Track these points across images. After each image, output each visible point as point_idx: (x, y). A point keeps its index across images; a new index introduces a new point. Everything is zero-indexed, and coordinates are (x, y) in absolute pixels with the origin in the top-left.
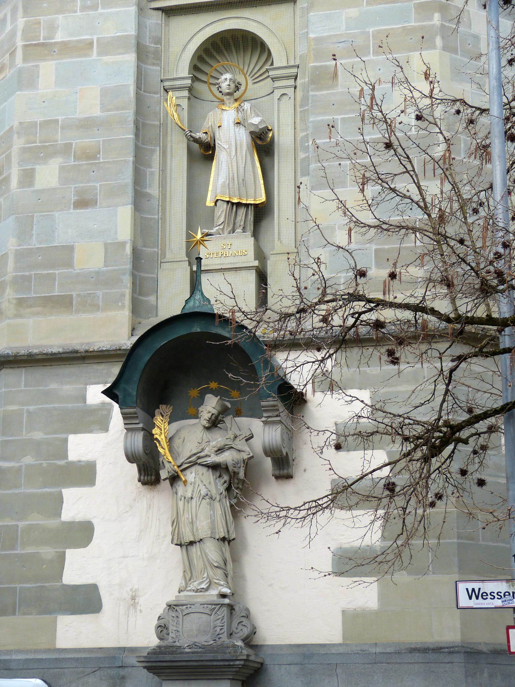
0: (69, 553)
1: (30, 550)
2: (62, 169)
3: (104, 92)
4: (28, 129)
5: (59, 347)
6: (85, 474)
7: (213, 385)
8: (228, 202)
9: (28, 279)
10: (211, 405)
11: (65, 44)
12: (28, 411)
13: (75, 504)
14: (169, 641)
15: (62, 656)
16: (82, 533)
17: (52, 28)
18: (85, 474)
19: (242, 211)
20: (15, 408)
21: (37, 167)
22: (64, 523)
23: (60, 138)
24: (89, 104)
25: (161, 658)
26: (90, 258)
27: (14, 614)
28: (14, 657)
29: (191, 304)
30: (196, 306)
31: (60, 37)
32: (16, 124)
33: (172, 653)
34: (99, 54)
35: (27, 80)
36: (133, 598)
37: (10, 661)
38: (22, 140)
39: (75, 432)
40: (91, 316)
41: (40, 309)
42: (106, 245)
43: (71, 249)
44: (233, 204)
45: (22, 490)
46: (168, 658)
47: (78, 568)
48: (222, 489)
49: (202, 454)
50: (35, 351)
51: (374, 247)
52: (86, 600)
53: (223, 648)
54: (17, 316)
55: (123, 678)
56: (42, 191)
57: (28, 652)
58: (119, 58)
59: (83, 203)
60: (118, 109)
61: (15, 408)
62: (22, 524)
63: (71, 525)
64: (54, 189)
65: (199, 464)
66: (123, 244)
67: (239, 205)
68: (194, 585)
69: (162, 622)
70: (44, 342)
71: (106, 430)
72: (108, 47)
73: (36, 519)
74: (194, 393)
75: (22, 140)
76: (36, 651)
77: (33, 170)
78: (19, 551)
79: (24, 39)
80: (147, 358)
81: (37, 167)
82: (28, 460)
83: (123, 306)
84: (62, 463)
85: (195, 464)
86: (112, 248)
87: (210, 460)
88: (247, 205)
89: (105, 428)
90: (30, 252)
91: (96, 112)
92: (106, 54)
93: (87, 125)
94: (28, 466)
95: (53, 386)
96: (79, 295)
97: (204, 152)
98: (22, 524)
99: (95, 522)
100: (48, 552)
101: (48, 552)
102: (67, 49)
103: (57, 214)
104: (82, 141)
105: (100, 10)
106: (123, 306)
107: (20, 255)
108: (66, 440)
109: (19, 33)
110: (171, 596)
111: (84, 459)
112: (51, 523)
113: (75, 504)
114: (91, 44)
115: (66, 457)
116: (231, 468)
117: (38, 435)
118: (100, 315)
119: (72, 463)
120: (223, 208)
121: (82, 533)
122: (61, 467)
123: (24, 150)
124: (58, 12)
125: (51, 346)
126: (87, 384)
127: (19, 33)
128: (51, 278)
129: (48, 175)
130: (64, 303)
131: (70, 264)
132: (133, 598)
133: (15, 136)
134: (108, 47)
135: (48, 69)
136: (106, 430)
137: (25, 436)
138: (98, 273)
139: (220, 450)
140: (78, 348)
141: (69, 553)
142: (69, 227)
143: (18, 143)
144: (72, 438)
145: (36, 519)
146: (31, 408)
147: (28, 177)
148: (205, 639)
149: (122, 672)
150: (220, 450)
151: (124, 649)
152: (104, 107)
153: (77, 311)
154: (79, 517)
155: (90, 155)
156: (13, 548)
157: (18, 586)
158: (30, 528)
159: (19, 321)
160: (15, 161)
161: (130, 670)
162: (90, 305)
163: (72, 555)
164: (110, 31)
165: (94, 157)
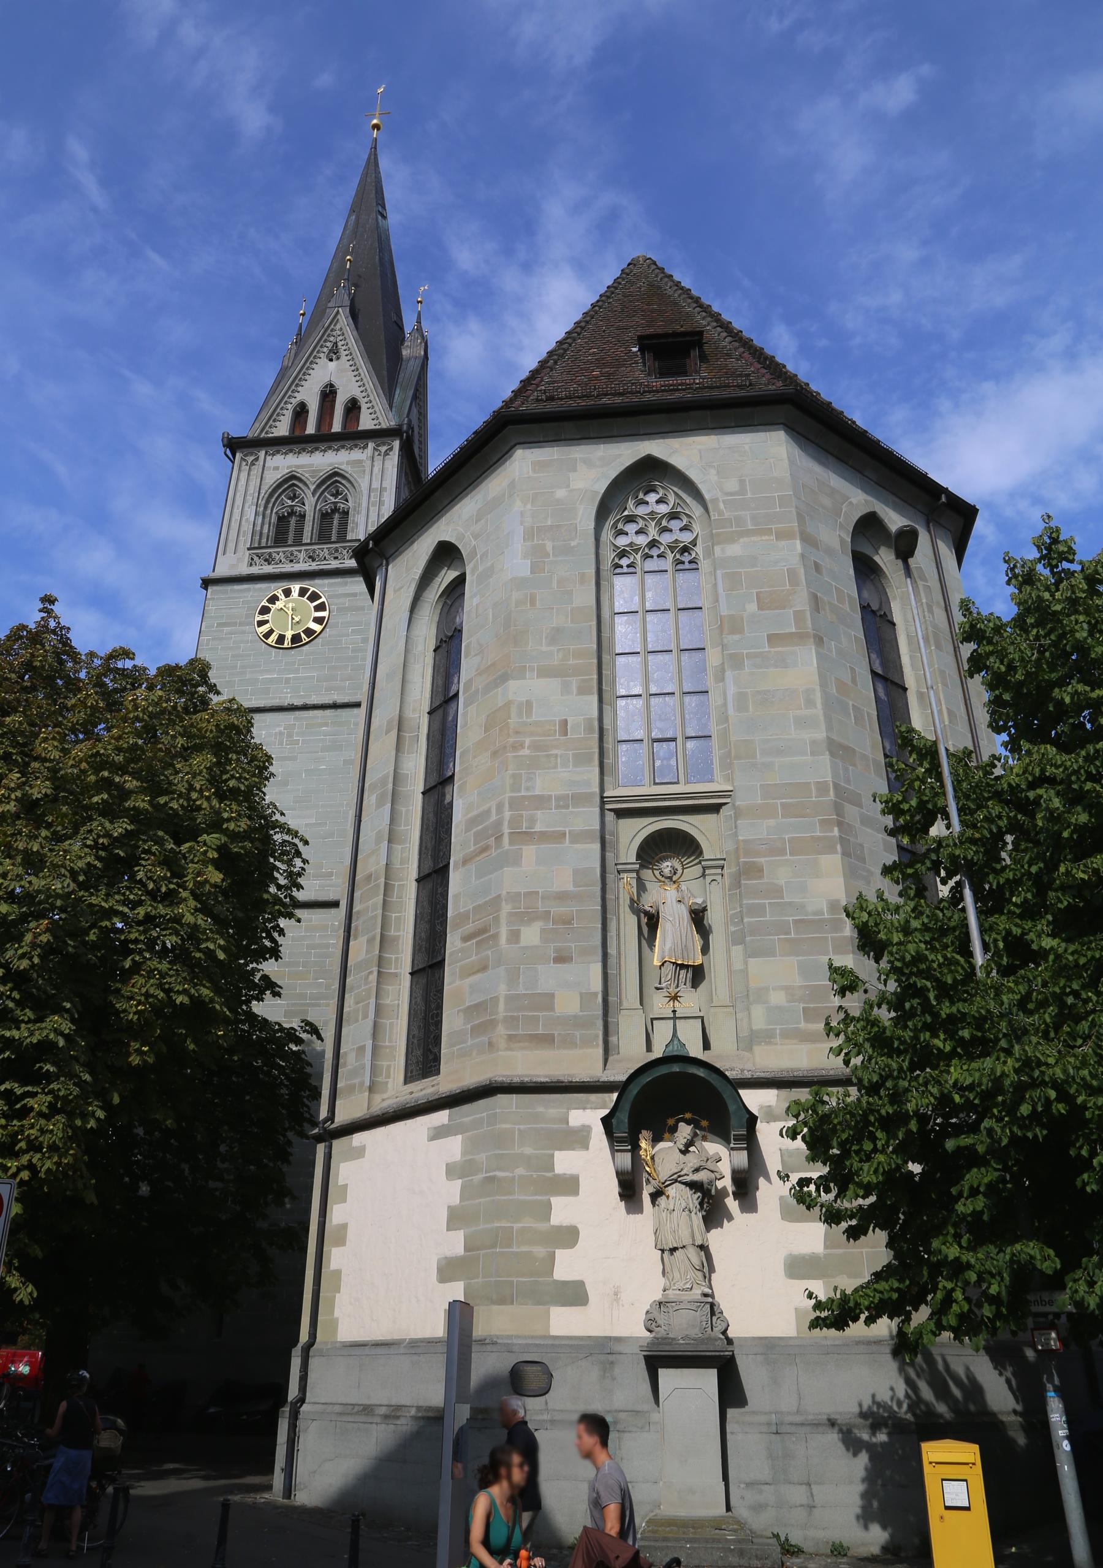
0: (560, 1254)
2: (543, 931)
3: (576, 872)
4: (514, 897)
5: (546, 1076)
6: (570, 1185)
7: (688, 1116)
8: (674, 963)
9: (517, 1018)
10: (685, 1131)
11: (542, 833)
12: (519, 1130)
13: (563, 1210)
14: (661, 1332)
15: (557, 1342)
16: (569, 1236)
17: (532, 821)
18: (570, 1185)
19: (683, 972)
20: (508, 1126)
21: (522, 928)
23: (541, 907)
24: (564, 881)
25: (661, 1348)
26: (568, 1004)
27: (512, 1303)
28: (515, 1341)
29: (671, 1048)
30: (675, 1050)
31: (538, 828)
32: (504, 892)
33: (670, 1344)
34: (571, 842)
35: (515, 860)
36: (616, 1294)
37: (513, 1344)
39: (560, 1150)
41: (527, 1044)
42: (581, 994)
43: (552, 996)
44: (677, 965)
46: (667, 1348)
47: (567, 1266)
48: (697, 1203)
49: (682, 1173)
50: (526, 1079)
51: (802, 1005)
52: (574, 1294)
53: (710, 1339)
54: (507, 1049)
55: (612, 1363)
57: (525, 1337)
59: (562, 958)
60: (587, 886)
61: (508, 1126)
63: (559, 1229)
64: (537, 947)
65: (680, 1182)
66: (596, 994)
67: (682, 966)
68: (680, 1285)
69: (651, 1316)
70: (532, 1072)
71: (587, 1149)
72: (578, 837)
73: (528, 1223)
74: (671, 1122)
76: (533, 1337)
77: (519, 930)
78: (515, 1249)
79: (510, 827)
80: (635, 1092)
81: (522, 928)
82: (520, 1171)
83: (598, 1045)
84: (549, 1175)
85: (676, 1181)
86: (586, 997)
87: (688, 1179)
88: (687, 967)
91: (570, 887)
93: (562, 897)
95: (540, 1109)
96: (559, 1034)
97: (651, 922)
99: (580, 1226)
100: (540, 1251)
101: (540, 1251)
102: (544, 837)
103: (539, 967)
104: (557, 909)
105: (571, 809)
106: (598, 1045)
107: (509, 999)
108: (553, 1156)
109: (506, 823)
110: (658, 1296)
111: (568, 1172)
112: (542, 1226)
113: (563, 1210)
116: (706, 1186)
117: (528, 1150)
119: (558, 1175)
120: (669, 968)
121: (569, 1236)
123: (511, 914)
124: (537, 809)
125: (539, 1076)
126: (569, 1109)
127: (506, 823)
128: (537, 1018)
129: (531, 935)
130: (546, 1040)
131: (551, 1008)
132: (616, 1294)
134: (578, 837)
135: (529, 852)
136: (586, 1147)
138: (575, 1017)
139: (697, 1170)
140: (562, 1079)
141: (560, 1254)
142: (549, 977)
143: (506, 909)
144: (557, 1154)
145: (528, 1223)
146: (522, 1127)
147: (515, 936)
148: (695, 1333)
149: (611, 1358)
150: (697, 1170)
151: (610, 1338)
152: (575, 885)
154: (566, 1223)
155: (567, 921)
156: (510, 1246)
157: (515, 1280)
159: (509, 1053)
160: (503, 921)
161: (618, 1356)
162: (569, 1042)
163: (562, 1256)
164: (579, 825)
165: (569, 923)
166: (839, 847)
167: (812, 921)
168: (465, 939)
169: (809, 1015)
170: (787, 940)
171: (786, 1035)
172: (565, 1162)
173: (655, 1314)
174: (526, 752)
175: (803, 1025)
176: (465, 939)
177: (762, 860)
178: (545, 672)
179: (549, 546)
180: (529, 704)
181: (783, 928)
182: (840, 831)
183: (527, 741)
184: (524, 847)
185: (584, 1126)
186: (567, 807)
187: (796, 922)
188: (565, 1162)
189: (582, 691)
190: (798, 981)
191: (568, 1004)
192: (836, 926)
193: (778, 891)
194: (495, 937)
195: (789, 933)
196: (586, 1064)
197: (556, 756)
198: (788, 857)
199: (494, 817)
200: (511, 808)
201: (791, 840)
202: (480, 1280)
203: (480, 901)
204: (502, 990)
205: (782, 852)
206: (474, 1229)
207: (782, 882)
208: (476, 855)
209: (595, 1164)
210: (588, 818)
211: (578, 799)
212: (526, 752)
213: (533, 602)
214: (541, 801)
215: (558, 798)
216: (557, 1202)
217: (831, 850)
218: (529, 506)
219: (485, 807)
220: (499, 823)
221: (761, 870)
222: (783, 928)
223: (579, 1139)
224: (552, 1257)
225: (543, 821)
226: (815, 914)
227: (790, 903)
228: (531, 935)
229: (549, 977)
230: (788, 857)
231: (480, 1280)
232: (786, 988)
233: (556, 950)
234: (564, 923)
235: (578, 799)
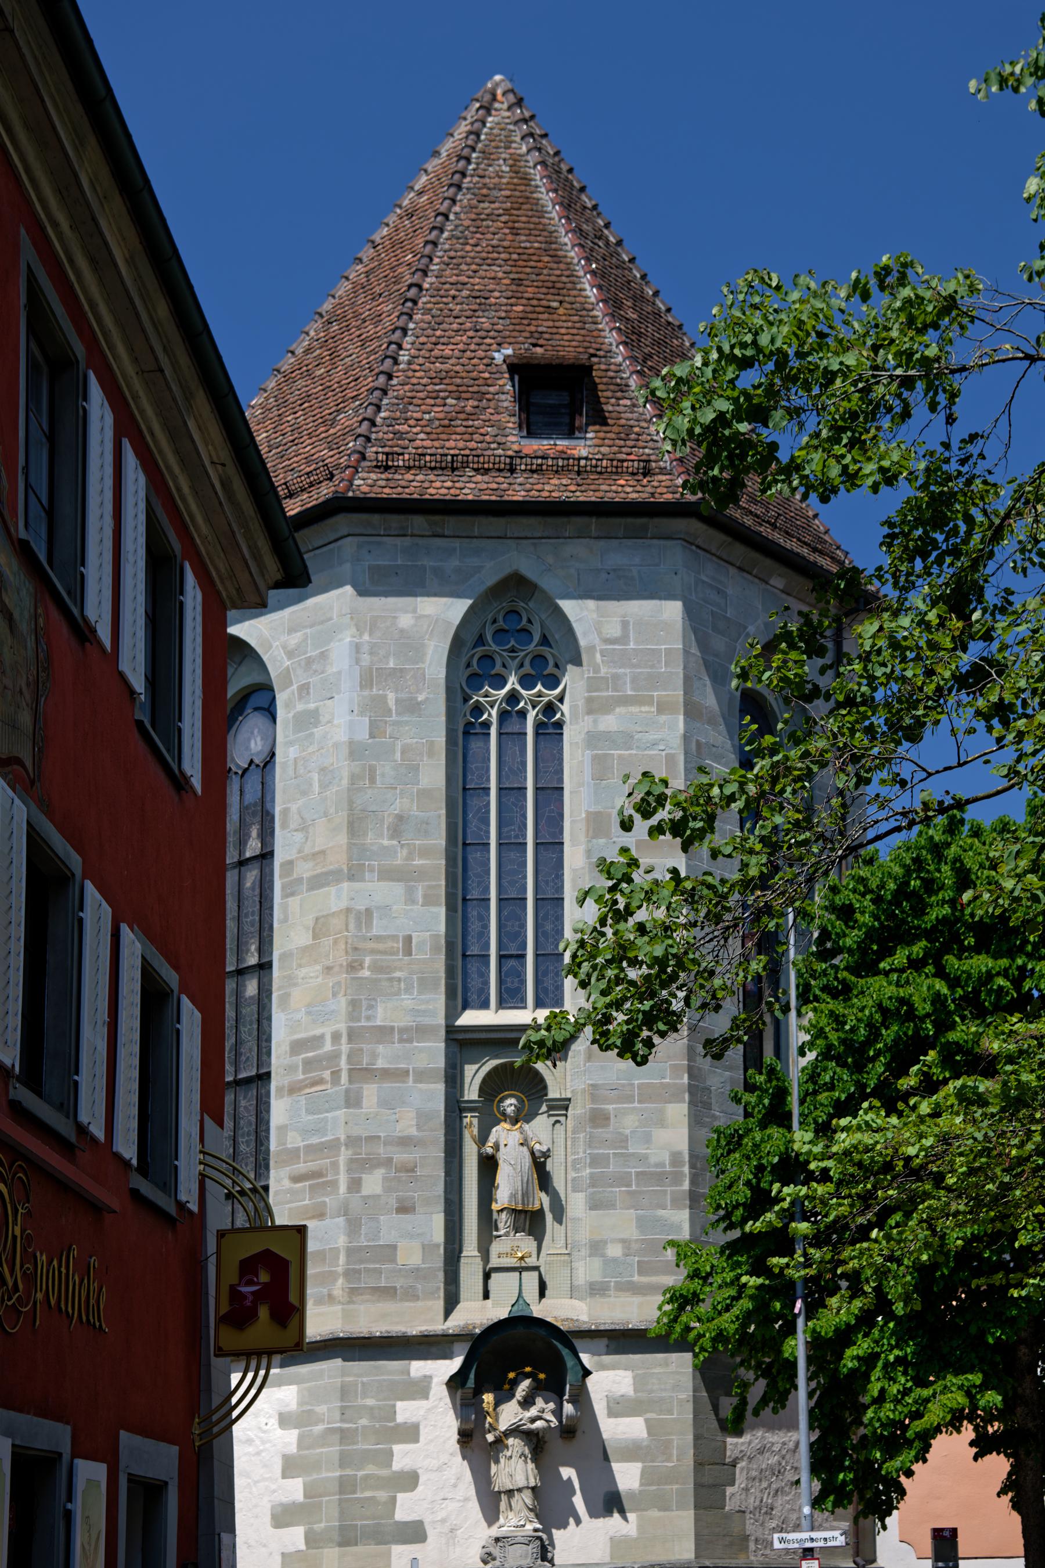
0: (400, 1496)
1: (368, 1494)
2: (385, 1179)
6: (411, 1433)
9: (359, 1271)
12: (363, 1383)
13: (403, 1456)
16: (410, 1480)
17: (374, 1056)
18: (411, 1433)
22: (395, 1472)
23: (382, 1151)
24: (407, 1124)
26: (410, 1255)
27: (356, 1544)
31: (380, 1064)
34: (415, 1082)
38: (350, 1152)
40: (412, 1304)
42: (424, 1247)
43: (394, 1248)
45: (359, 1446)
56: (368, 1197)
58: (432, 1086)
59: (404, 1208)
62: (360, 1473)
64: (379, 1196)
66: (438, 1246)
71: (427, 1398)
72: (421, 1076)
73: (370, 1470)
75: (350, 1152)
77: (360, 1179)
82: (364, 1422)
86: (427, 1249)
89: (425, 1396)
90: (360, 1249)
91: (413, 1131)
92: (421, 1082)
93: (405, 1142)
94: (364, 1427)
98: (360, 1473)
99: (420, 1471)
100: (382, 1495)
102: (386, 1074)
104: (401, 1156)
112: (384, 1472)
113: (403, 1456)
114: (407, 1072)
115: (394, 1420)
117: (370, 1402)
118: (420, 1304)
121: (410, 1480)
122: (392, 1428)
124: (379, 1042)
128: (380, 1272)
129: (373, 1183)
130: (388, 1293)
131: (393, 1260)
133: (343, 1148)
134: (421, 1076)
136: (427, 1398)
137: (360, 1402)
141: (400, 1496)
142: (390, 1228)
144: (400, 1405)
145: (370, 1470)
147: (355, 1185)
152: (419, 1127)
153: (401, 1300)
156: (355, 1492)
158: (366, 1478)
159: (351, 1307)
160: (342, 1168)
162: (411, 1295)
164: (422, 1062)
165: (413, 1170)
166: (687, 1096)
167: (652, 1174)
168: (296, 1179)
169: (643, 1269)
170: (629, 1192)
171: (621, 1287)
172: (406, 1411)
173: (491, 1549)
174: (366, 973)
175: (636, 1278)
176: (296, 1179)
177: (610, 1107)
178: (388, 875)
179: (391, 697)
180: (368, 912)
181: (623, 1180)
182: (689, 1078)
183: (368, 960)
184: (365, 1086)
185: (425, 1376)
186: (410, 1041)
187: (638, 1174)
188: (406, 1411)
189: (428, 901)
190: (632, 1232)
191: (410, 1255)
192: (677, 1178)
193: (623, 1141)
194: (334, 1184)
195: (630, 1186)
196: (425, 1318)
197: (399, 980)
198: (636, 1105)
199: (328, 1047)
200: (350, 1039)
201: (640, 1086)
202: (323, 1525)
203: (315, 1140)
204: (342, 1241)
205: (630, 1099)
206: (315, 1476)
207: (627, 1132)
208: (306, 1086)
209: (436, 1417)
210: (433, 1053)
211: (422, 1031)
212: (366, 973)
213: (372, 780)
214: (384, 1033)
215: (402, 1030)
216: (397, 1448)
217: (676, 1098)
218: (366, 637)
219: (318, 1032)
220: (335, 1056)
221: (608, 1119)
222: (623, 1180)
223: (420, 1389)
224: (394, 1500)
225: (384, 1056)
226: (657, 1165)
227: (633, 1154)
228: (373, 1183)
229: (390, 1228)
230: (636, 1105)
231: (323, 1525)
232: (623, 1241)
233: (398, 1200)
234: (407, 1171)
235: (422, 1031)
